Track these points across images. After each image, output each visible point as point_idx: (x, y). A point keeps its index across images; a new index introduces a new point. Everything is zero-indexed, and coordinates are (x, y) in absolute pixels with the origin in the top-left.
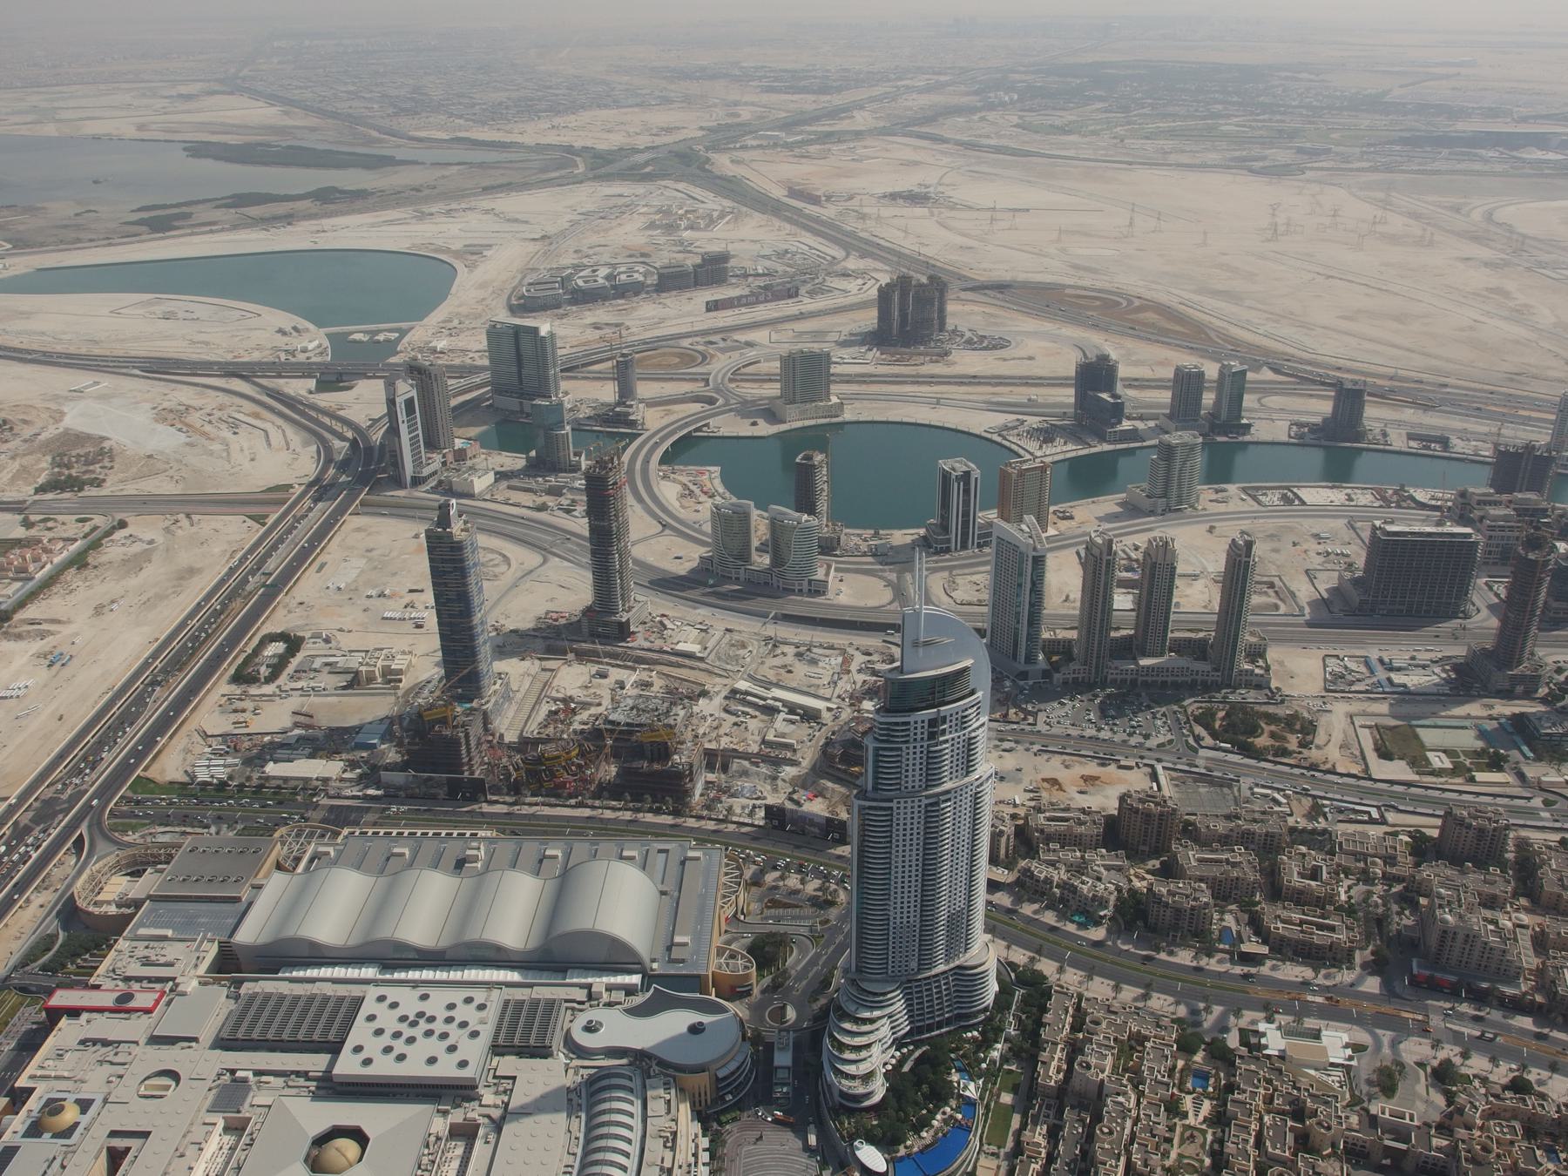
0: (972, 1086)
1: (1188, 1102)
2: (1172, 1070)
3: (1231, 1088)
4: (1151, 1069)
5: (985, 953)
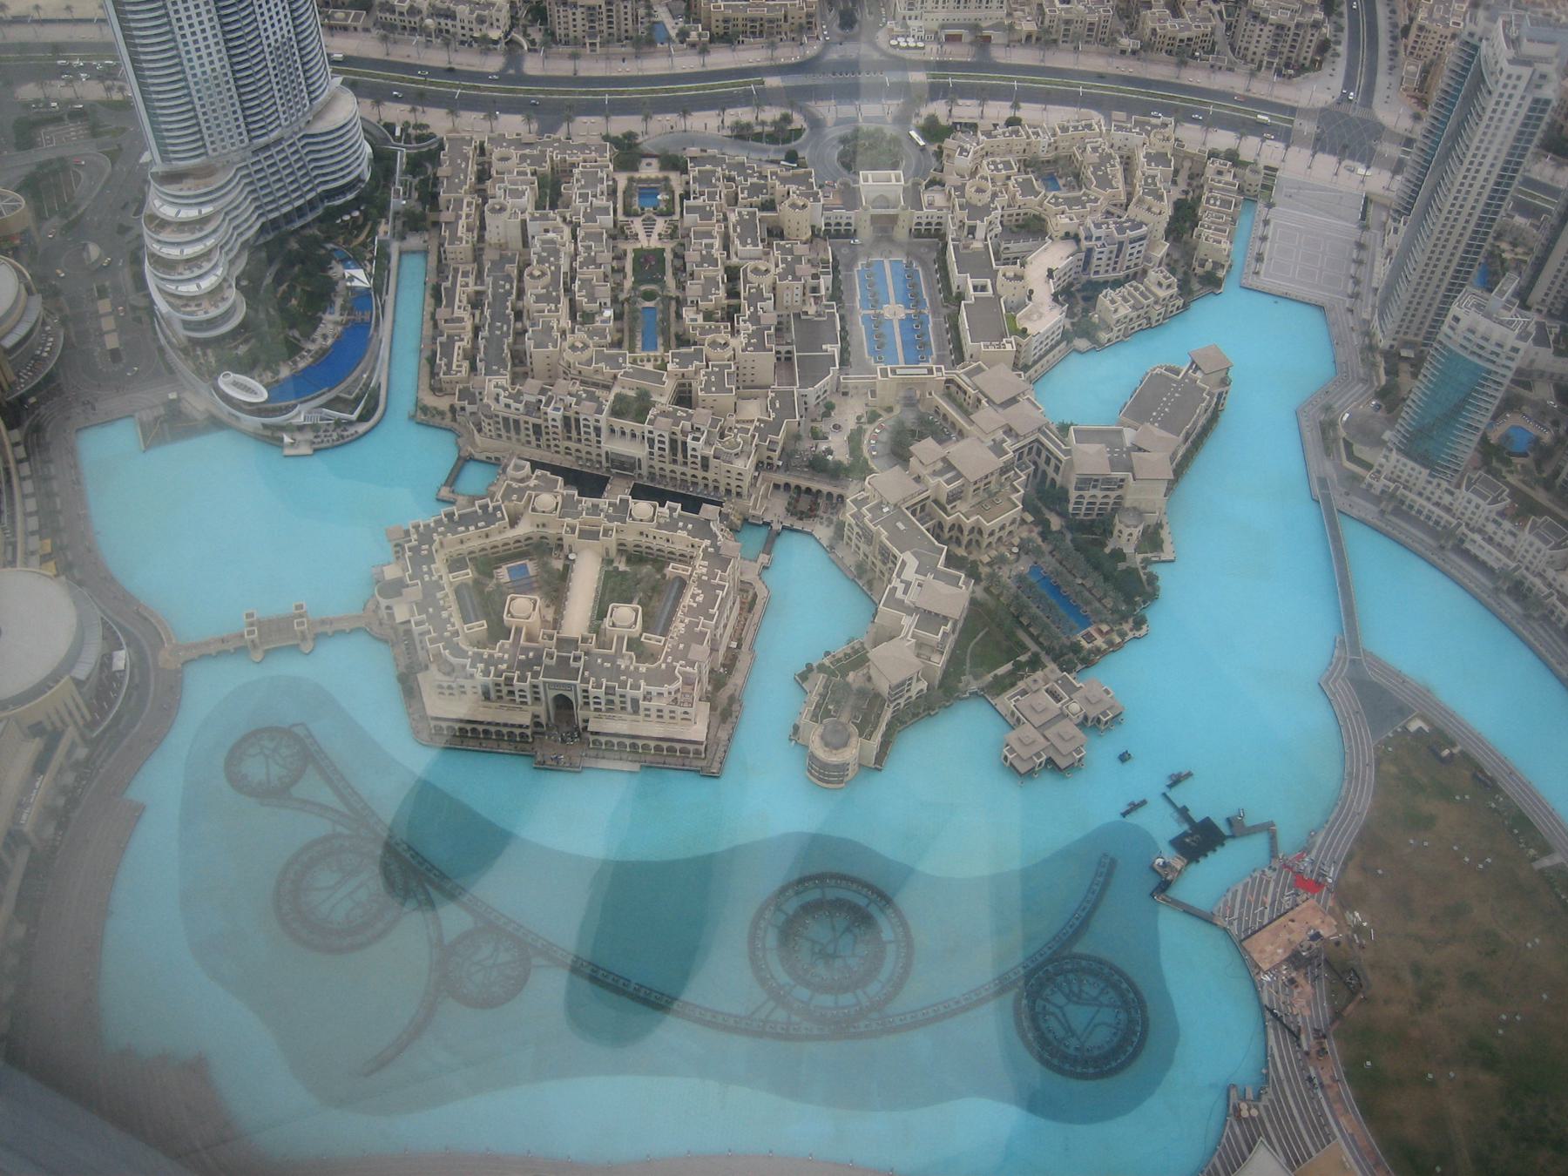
0: (359, 273)
1: (637, 225)
2: (612, 193)
3: (686, 195)
4: (584, 197)
5: (346, 109)
